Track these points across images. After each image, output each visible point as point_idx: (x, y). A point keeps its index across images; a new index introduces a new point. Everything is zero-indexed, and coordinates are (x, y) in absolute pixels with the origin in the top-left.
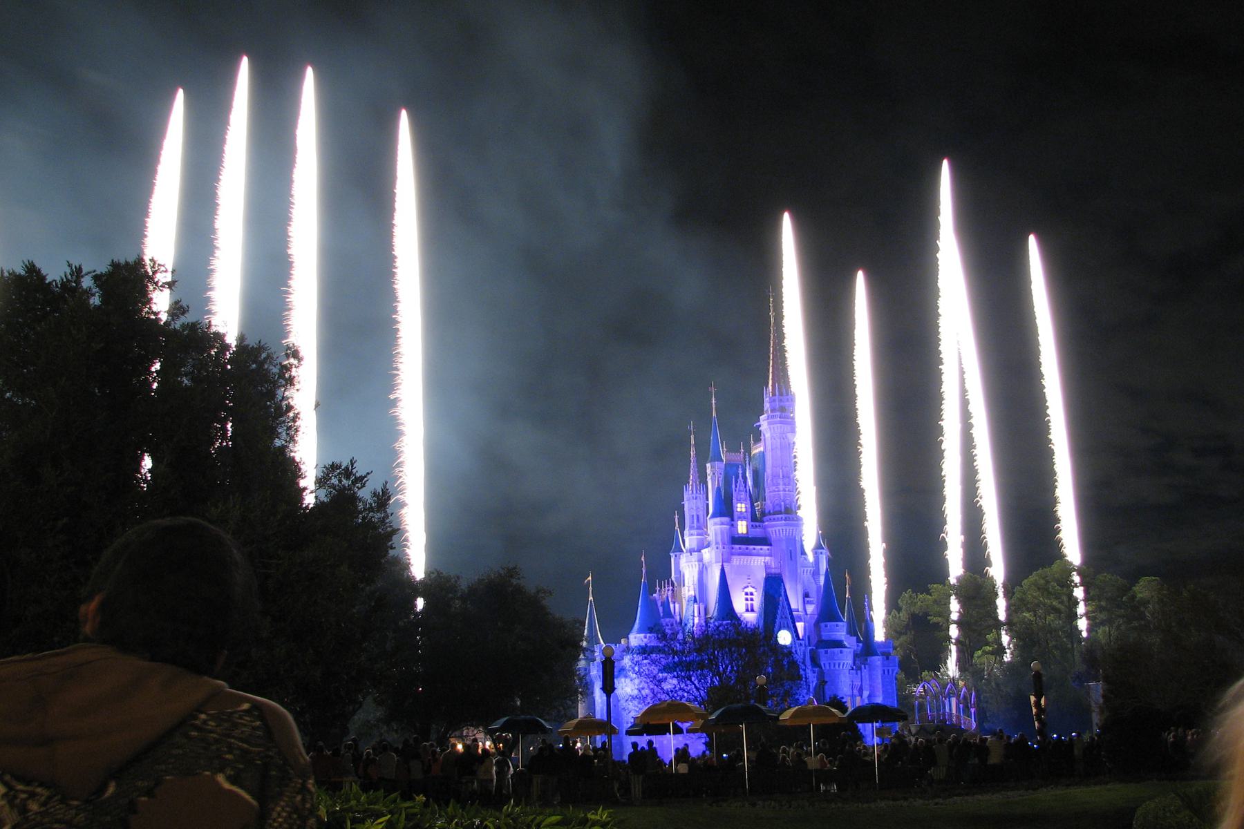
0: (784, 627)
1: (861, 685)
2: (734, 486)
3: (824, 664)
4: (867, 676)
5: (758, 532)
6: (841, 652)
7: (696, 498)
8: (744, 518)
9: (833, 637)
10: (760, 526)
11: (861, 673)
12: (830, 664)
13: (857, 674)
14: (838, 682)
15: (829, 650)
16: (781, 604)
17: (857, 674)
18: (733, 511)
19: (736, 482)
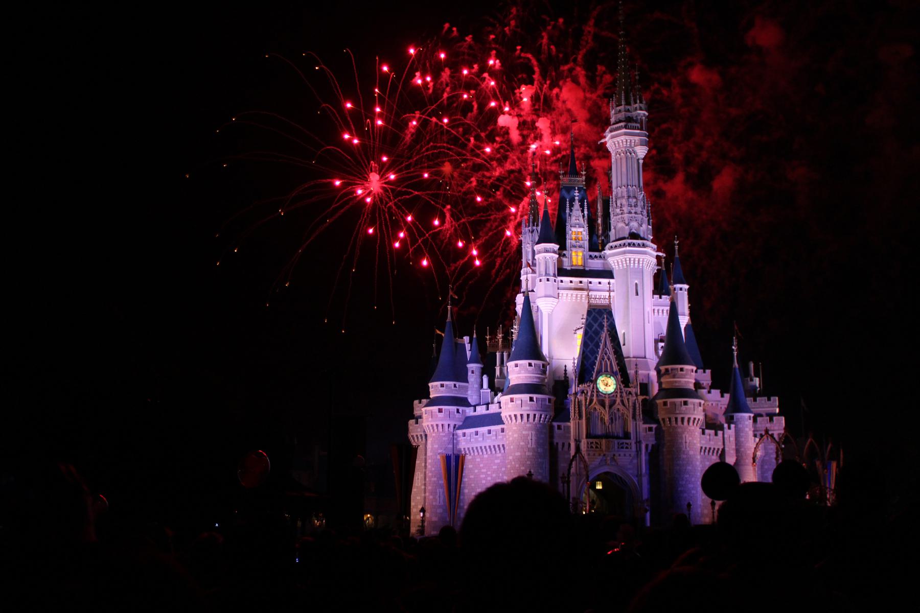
0: (606, 371)
1: (723, 450)
2: (568, 211)
3: (663, 419)
4: (732, 439)
5: (596, 264)
6: (685, 403)
7: (533, 231)
8: (580, 247)
9: (677, 384)
10: (600, 257)
11: (723, 434)
12: (670, 419)
13: (716, 434)
14: (682, 443)
15: (669, 401)
16: (603, 341)
17: (716, 434)
18: (565, 239)
19: (571, 206)
